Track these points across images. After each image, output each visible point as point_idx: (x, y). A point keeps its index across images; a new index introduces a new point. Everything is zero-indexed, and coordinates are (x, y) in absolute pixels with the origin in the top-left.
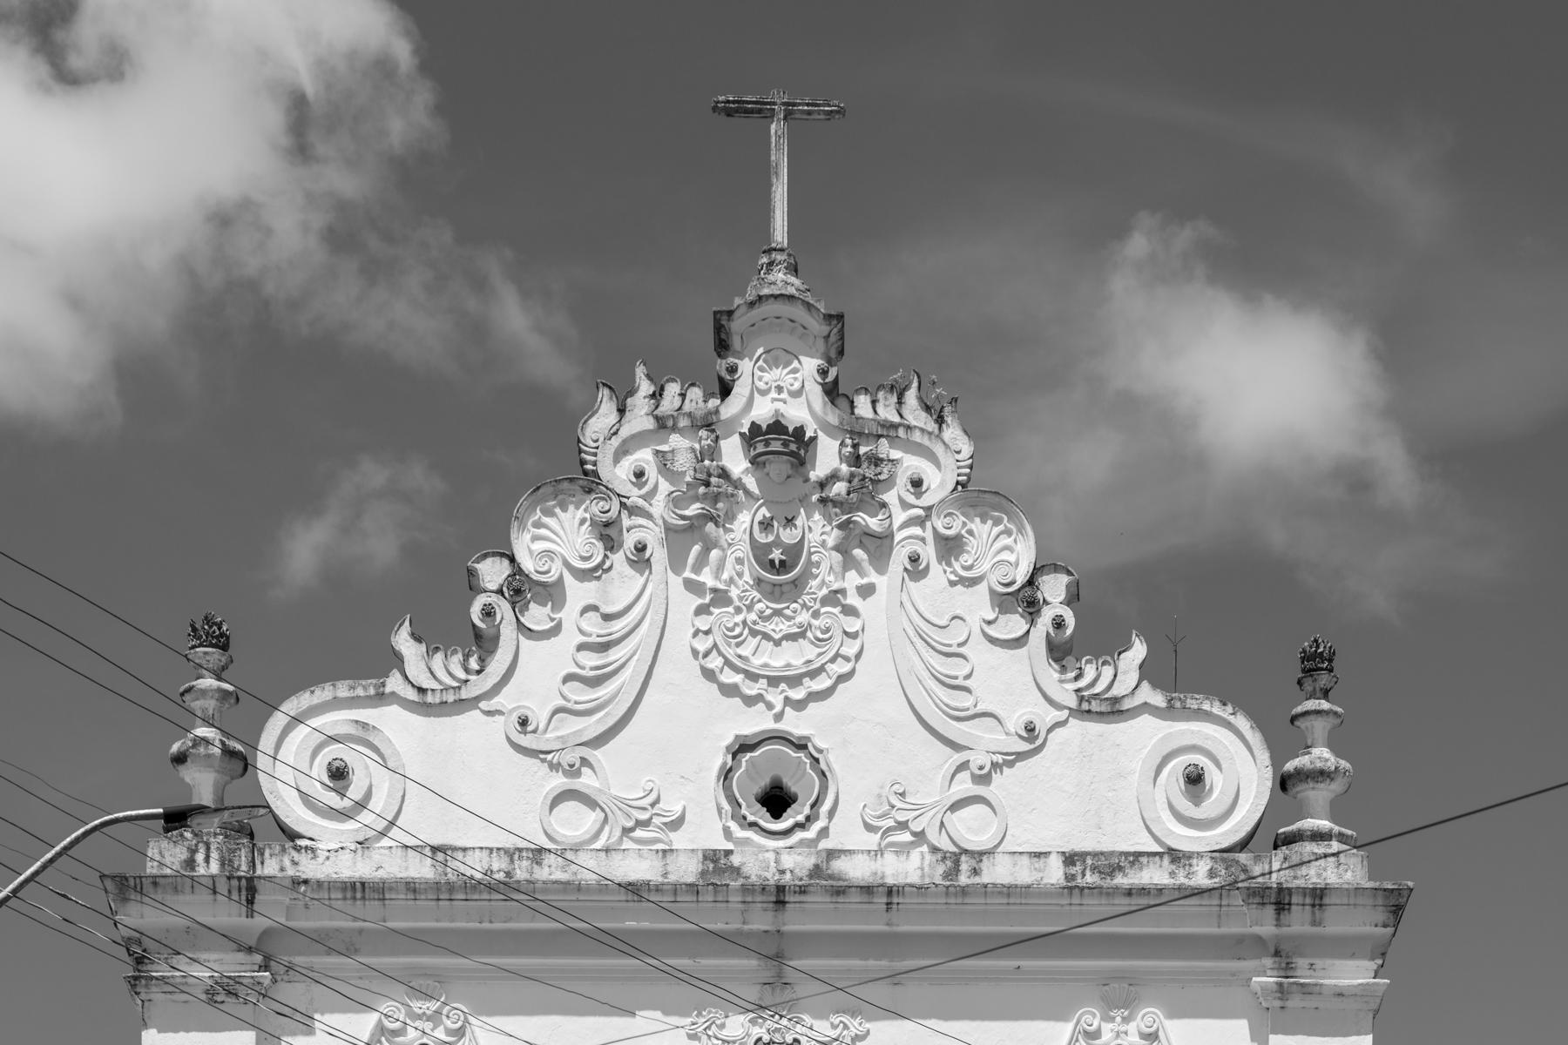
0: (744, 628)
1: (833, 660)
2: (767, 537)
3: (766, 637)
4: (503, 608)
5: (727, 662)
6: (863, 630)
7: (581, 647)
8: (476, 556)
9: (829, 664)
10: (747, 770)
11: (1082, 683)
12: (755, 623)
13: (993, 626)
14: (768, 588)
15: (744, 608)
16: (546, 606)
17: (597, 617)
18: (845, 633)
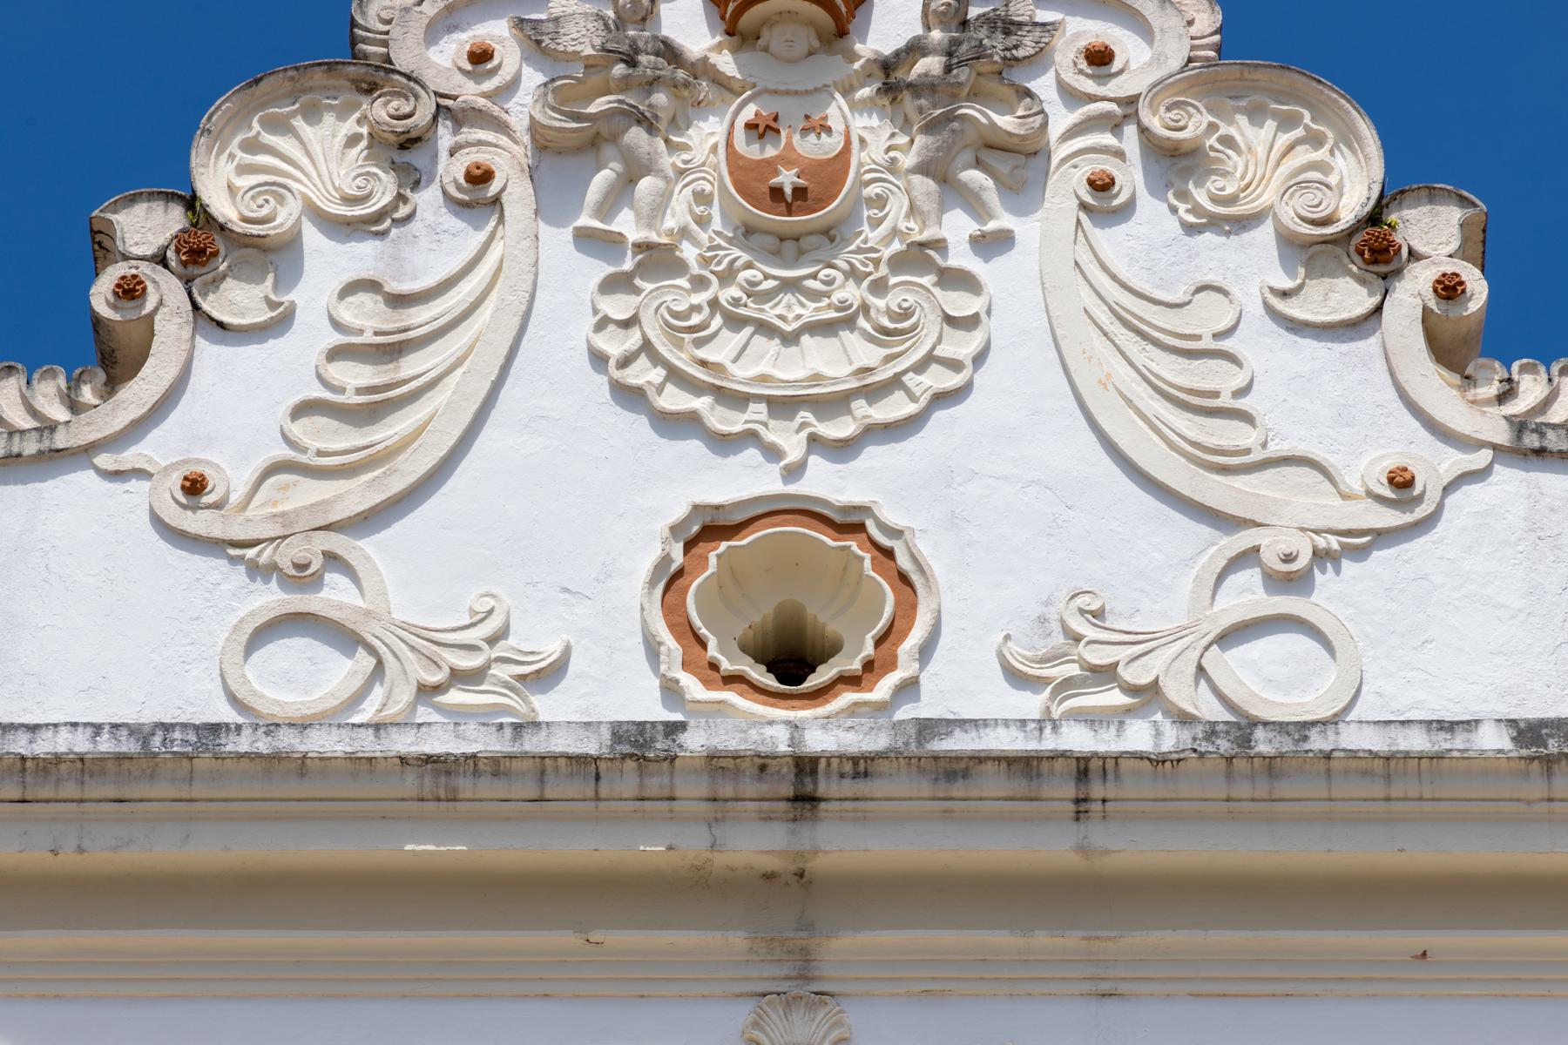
0: (712, 316)
1: (920, 367)
2: (762, 150)
3: (765, 328)
4: (166, 290)
5: (675, 376)
6: (989, 312)
7: (335, 354)
8: (117, 197)
9: (911, 374)
10: (717, 575)
11: (1518, 406)
12: (736, 302)
13: (1294, 301)
14: (770, 241)
15: (714, 279)
16: (263, 280)
17: (376, 302)
18: (950, 320)
